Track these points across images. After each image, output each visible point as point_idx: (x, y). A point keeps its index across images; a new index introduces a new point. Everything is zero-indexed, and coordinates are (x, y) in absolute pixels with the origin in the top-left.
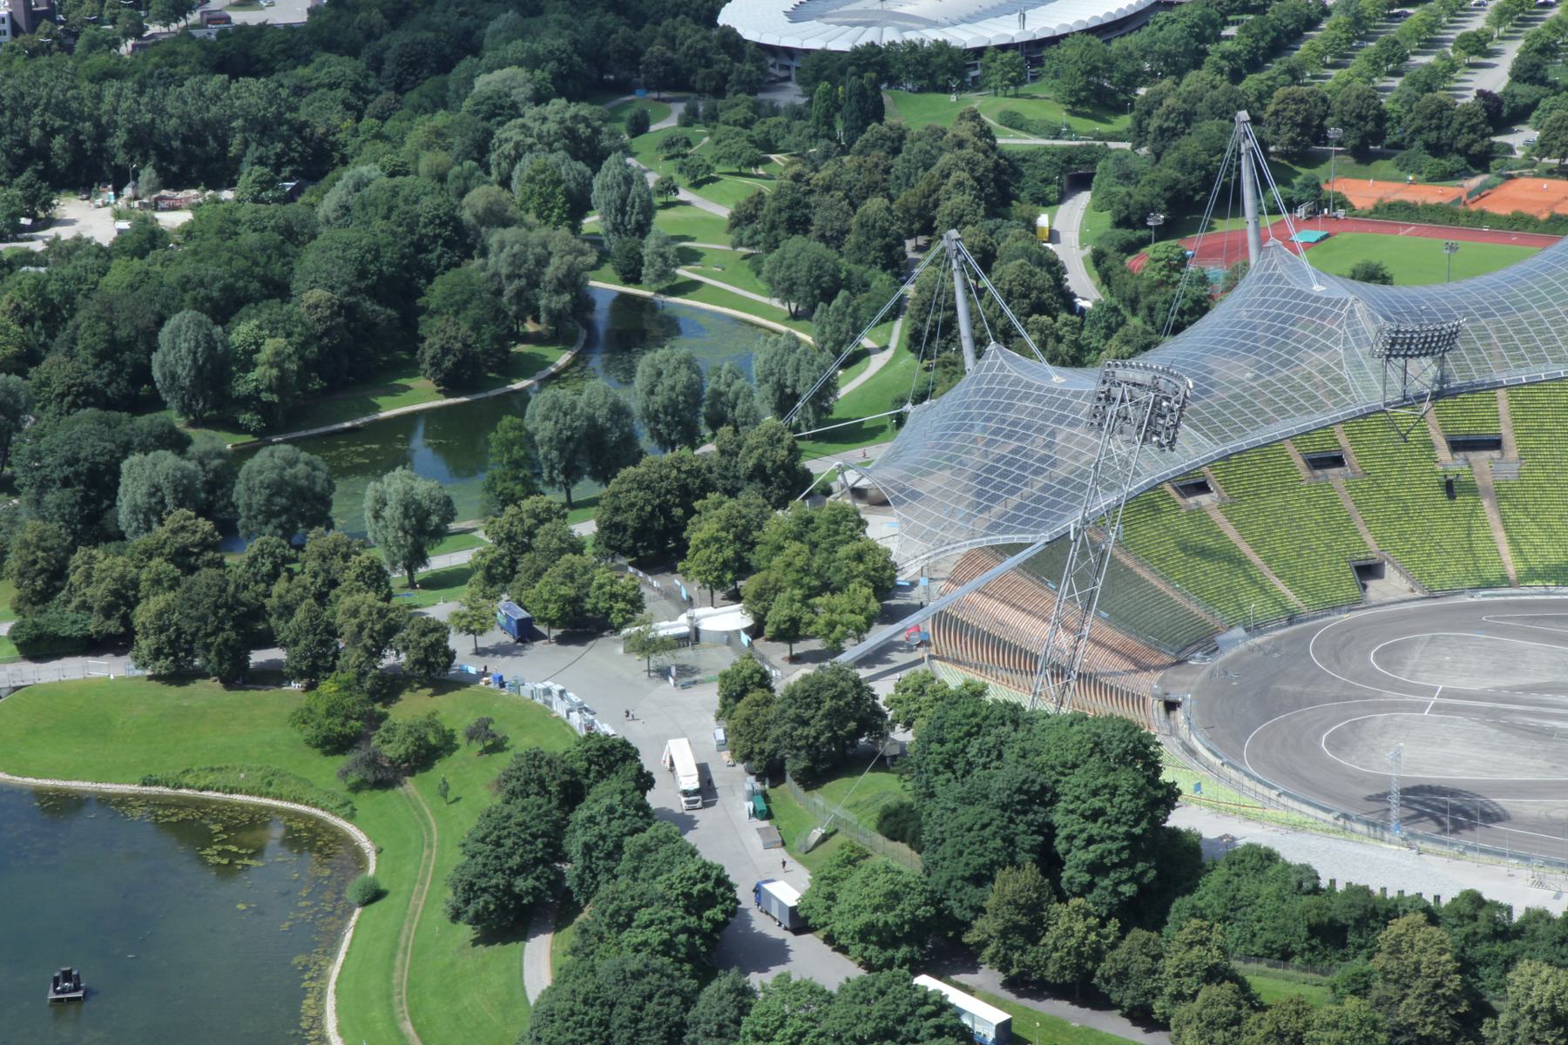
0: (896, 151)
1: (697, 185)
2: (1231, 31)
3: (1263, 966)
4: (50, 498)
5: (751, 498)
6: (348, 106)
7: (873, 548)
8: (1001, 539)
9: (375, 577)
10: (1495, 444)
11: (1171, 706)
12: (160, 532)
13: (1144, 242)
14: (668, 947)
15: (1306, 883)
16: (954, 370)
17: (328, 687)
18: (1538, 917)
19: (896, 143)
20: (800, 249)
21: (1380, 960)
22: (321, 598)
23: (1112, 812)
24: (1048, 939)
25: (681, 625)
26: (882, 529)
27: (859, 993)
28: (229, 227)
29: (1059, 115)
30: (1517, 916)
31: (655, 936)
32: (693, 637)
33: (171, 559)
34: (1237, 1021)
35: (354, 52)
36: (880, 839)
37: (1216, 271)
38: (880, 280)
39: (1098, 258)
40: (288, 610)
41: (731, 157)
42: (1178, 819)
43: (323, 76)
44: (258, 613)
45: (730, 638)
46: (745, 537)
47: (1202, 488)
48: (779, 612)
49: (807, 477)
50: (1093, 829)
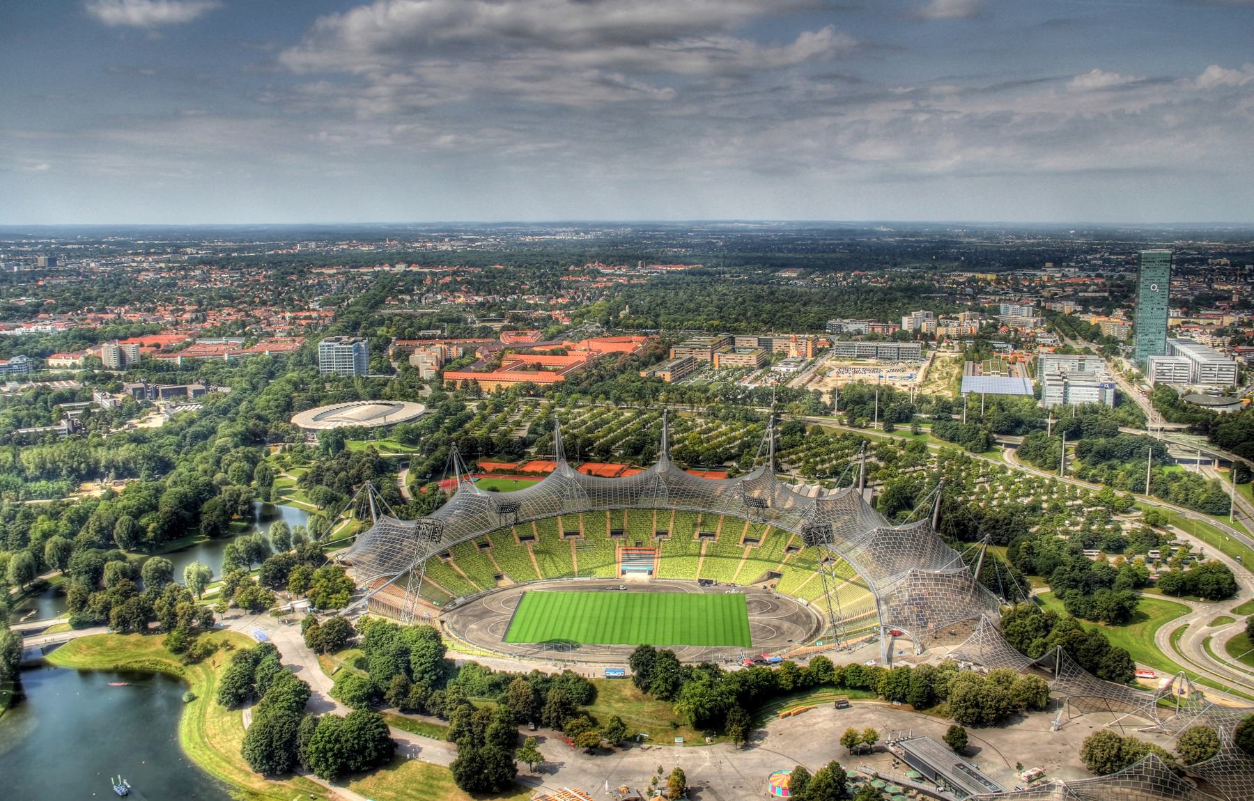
0: (348, 458)
1: (287, 471)
2: (447, 421)
3: (476, 698)
4: (82, 578)
5: (308, 566)
6: (175, 451)
7: (348, 579)
8: (388, 574)
9: (188, 597)
10: (533, 538)
11: (442, 622)
12: (118, 586)
13: (426, 483)
14: (290, 708)
15: (487, 672)
16: (370, 524)
17: (175, 633)
18: (555, 675)
19: (348, 455)
20: (321, 489)
21: (510, 692)
22: (171, 604)
23: (428, 655)
24: (410, 695)
25: (288, 607)
26: (350, 573)
27: (353, 717)
28: (139, 490)
29: (398, 447)
30: (549, 675)
31: (285, 704)
32: (293, 610)
33: (121, 595)
34: (470, 715)
35: (177, 434)
36: (356, 669)
37: (448, 491)
38: (346, 497)
39: (412, 488)
40: (161, 609)
41: (297, 462)
42: (448, 655)
43: (167, 442)
44: (151, 610)
45: (304, 610)
46: (307, 577)
47: (448, 555)
48: (320, 600)
49: (326, 558)
50: (423, 660)
